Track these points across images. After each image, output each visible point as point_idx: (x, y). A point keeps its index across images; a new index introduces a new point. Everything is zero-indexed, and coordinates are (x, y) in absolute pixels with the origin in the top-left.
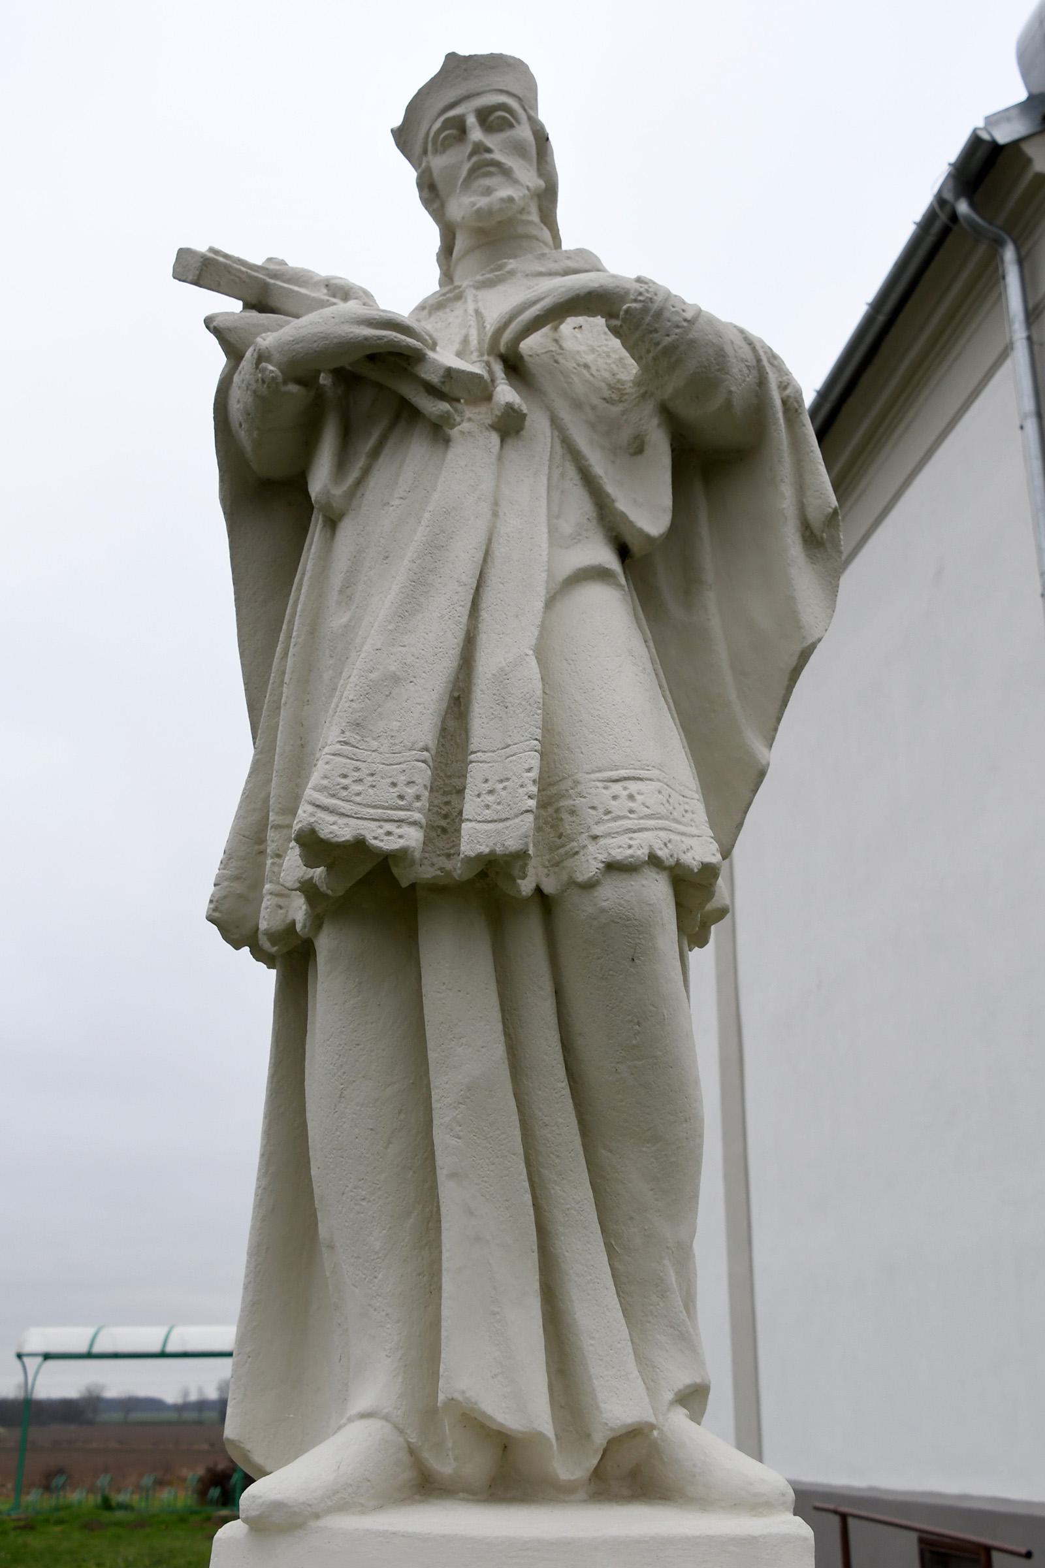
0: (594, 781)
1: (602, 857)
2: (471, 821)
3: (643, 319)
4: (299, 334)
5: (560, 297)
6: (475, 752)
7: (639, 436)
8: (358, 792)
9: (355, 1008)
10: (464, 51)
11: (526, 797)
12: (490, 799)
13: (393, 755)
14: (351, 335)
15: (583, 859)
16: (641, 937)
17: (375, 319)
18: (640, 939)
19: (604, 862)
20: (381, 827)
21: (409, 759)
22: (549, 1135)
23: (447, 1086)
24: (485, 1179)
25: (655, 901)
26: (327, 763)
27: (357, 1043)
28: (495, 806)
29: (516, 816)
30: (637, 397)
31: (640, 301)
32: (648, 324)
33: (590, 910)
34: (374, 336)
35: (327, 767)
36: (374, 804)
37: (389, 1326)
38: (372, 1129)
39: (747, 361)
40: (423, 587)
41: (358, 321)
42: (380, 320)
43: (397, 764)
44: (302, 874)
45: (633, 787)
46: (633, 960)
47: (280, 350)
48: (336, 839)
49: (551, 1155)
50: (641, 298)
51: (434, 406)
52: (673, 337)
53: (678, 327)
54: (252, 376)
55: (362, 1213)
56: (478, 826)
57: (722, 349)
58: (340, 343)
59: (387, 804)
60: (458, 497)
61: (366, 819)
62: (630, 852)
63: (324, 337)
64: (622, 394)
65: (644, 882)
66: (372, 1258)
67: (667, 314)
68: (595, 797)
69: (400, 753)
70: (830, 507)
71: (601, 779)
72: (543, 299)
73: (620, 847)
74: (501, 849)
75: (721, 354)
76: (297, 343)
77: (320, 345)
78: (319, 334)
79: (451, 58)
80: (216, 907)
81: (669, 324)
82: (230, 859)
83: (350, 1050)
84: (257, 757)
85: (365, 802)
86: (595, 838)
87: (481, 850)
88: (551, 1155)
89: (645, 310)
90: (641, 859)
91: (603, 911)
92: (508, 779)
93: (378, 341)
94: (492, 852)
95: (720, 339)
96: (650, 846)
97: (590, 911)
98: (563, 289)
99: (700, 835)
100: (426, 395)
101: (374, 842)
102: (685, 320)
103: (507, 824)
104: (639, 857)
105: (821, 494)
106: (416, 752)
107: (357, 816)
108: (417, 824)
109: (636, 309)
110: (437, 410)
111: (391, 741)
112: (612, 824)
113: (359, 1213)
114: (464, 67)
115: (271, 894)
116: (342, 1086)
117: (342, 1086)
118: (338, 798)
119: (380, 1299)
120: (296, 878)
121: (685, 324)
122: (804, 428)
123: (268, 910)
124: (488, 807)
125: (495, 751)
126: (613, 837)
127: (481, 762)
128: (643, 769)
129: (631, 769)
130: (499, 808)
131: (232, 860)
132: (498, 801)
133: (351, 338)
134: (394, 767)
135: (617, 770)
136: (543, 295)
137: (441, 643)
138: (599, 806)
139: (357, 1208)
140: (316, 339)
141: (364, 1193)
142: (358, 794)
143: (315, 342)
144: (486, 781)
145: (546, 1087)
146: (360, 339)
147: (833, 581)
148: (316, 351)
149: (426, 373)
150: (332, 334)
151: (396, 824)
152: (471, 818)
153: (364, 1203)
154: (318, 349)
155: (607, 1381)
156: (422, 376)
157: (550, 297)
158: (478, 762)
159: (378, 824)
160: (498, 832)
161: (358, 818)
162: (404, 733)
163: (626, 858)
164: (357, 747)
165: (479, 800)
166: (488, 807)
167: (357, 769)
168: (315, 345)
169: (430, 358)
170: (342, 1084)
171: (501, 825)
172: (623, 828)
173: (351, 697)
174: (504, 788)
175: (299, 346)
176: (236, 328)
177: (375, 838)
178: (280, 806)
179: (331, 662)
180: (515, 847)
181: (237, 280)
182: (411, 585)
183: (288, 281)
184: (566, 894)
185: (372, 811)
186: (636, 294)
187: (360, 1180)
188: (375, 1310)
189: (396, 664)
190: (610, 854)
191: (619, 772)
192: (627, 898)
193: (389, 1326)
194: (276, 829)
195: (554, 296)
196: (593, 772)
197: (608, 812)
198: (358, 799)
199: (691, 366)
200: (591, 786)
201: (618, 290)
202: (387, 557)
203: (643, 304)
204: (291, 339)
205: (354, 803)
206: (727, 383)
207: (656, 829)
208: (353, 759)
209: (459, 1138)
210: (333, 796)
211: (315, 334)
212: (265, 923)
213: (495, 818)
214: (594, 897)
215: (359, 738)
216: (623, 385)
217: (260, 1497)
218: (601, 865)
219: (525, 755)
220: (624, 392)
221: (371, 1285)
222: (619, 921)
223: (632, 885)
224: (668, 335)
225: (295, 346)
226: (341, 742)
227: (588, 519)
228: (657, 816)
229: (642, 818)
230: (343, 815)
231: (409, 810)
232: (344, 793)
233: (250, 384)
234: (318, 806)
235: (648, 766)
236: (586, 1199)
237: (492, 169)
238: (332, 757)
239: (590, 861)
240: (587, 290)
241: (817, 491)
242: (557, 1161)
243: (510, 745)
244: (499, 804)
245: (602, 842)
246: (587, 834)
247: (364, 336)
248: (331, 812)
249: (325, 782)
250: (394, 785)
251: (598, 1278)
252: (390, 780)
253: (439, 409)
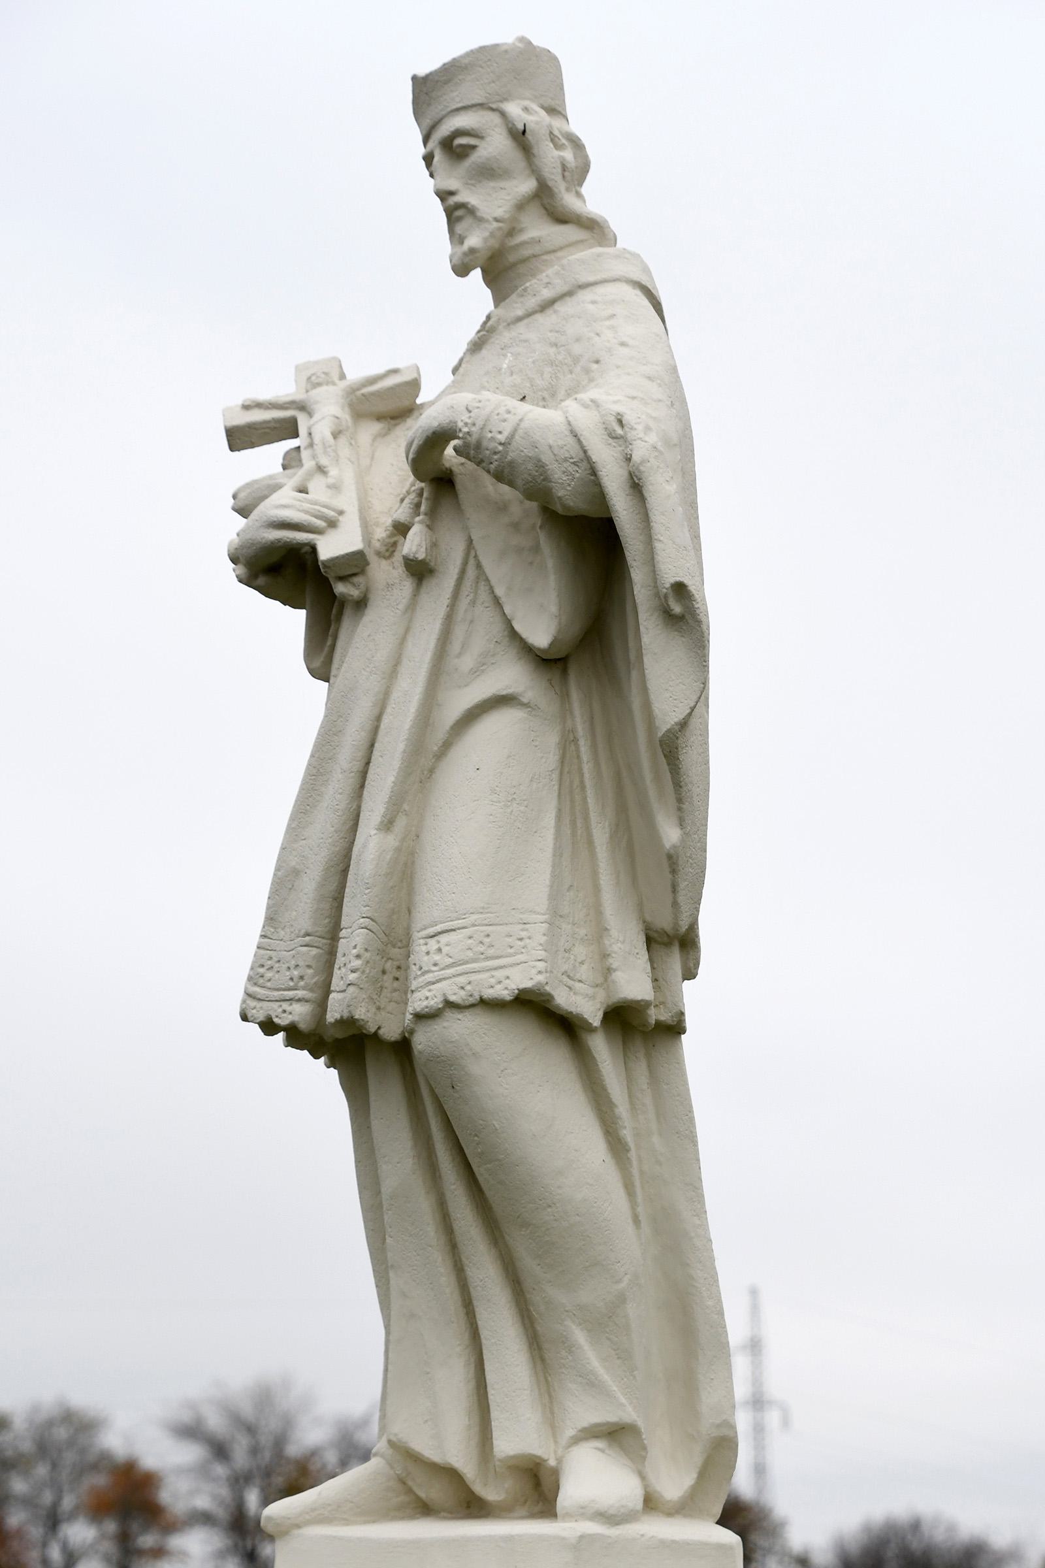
14: (264, 541)
16: (452, 1068)
17: (275, 522)
24: (415, 1268)
25: (457, 1038)
39: (572, 458)
45: (444, 939)
46: (453, 1087)
53: (495, 453)
57: (539, 461)
59: (283, 987)
60: (355, 676)
62: (425, 1003)
65: (445, 1024)
67: (485, 443)
70: (664, 588)
71: (424, 936)
73: (420, 1000)
75: (540, 465)
81: (488, 452)
85: (273, 986)
95: (536, 450)
102: (500, 444)
104: (432, 1007)
121: (500, 448)
128: (459, 919)
129: (448, 921)
135: (436, 925)
147: (699, 652)
151: (288, 1003)
155: (501, 1422)
161: (268, 1001)
163: (423, 1009)
164: (271, 939)
167: (270, 958)
172: (425, 982)
176: (247, 506)
177: (277, 1017)
181: (267, 430)
189: (296, 858)
191: (437, 927)
196: (422, 930)
198: (269, 984)
201: (451, 425)
207: (454, 976)
208: (268, 950)
215: (272, 930)
222: (432, 1059)
223: (435, 1029)
224: (491, 463)
227: (496, 642)
228: (459, 963)
229: (443, 969)
230: (260, 1000)
231: (296, 989)
232: (261, 981)
236: (487, 1277)
240: (431, 431)
251: (499, 1341)
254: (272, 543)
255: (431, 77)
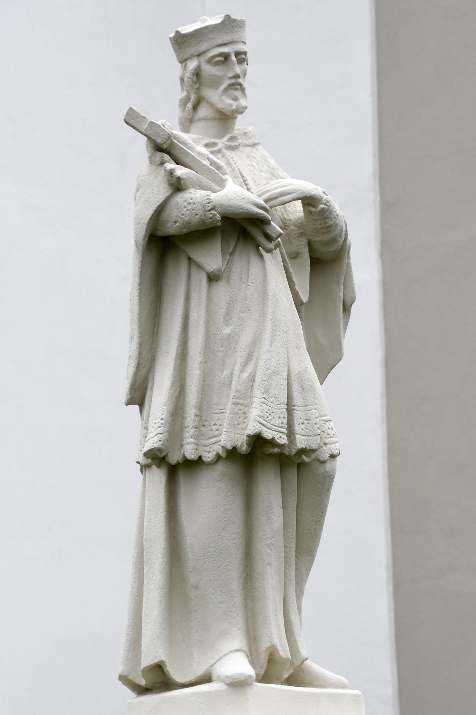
0: (322, 420)
1: (329, 452)
2: (298, 434)
3: (326, 213)
4: (230, 202)
5: (300, 195)
6: (295, 406)
7: (298, 252)
9: (231, 495)
10: (233, 17)
12: (303, 426)
13: (278, 405)
14: (252, 210)
15: (322, 452)
17: (259, 204)
19: (330, 454)
20: (278, 434)
21: (283, 408)
22: (288, 551)
23: (268, 530)
26: (261, 406)
27: (231, 509)
28: (305, 430)
29: (315, 436)
30: (298, 233)
31: (327, 205)
32: (327, 215)
33: (322, 471)
34: (260, 213)
35: (261, 408)
36: (275, 425)
37: (238, 618)
38: (235, 544)
41: (253, 204)
42: (261, 205)
43: (279, 409)
44: (233, 444)
46: (328, 490)
47: (221, 207)
48: (268, 438)
49: (288, 559)
50: (328, 204)
51: (268, 245)
52: (333, 222)
54: (203, 212)
55: (229, 575)
56: (301, 437)
58: (246, 212)
59: (279, 425)
61: (274, 430)
63: (242, 208)
64: (285, 225)
66: (232, 593)
67: (333, 212)
68: (323, 427)
69: (279, 405)
71: (324, 420)
72: (294, 193)
74: (309, 447)
76: (230, 207)
77: (239, 211)
78: (240, 206)
79: (227, 17)
80: (163, 444)
81: (333, 216)
82: (166, 423)
83: (229, 512)
84: (173, 379)
85: (273, 424)
86: (325, 444)
87: (302, 447)
88: (288, 559)
89: (328, 209)
91: (326, 472)
92: (309, 420)
93: (260, 216)
94: (306, 448)
97: (322, 471)
98: (301, 191)
100: (264, 238)
101: (277, 440)
103: (312, 438)
105: (354, 292)
107: (272, 429)
109: (325, 209)
110: (269, 247)
111: (276, 399)
112: (330, 439)
113: (227, 575)
114: (232, 25)
115: (194, 443)
116: (224, 526)
117: (224, 526)
118: (266, 421)
119: (234, 608)
120: (231, 445)
122: (349, 260)
123: (194, 450)
124: (303, 429)
125: (301, 407)
126: (331, 445)
127: (298, 410)
130: (307, 431)
131: (167, 424)
132: (306, 428)
133: (251, 212)
134: (279, 410)
136: (292, 192)
137: (284, 359)
138: (325, 431)
139: (227, 573)
140: (238, 208)
141: (230, 568)
142: (271, 420)
143: (238, 209)
144: (300, 419)
145: (289, 533)
146: (255, 213)
148: (237, 213)
149: (269, 231)
150: (245, 207)
152: (298, 433)
153: (230, 571)
154: (238, 212)
156: (268, 231)
157: (296, 193)
158: (297, 410)
160: (308, 440)
161: (272, 430)
162: (279, 396)
165: (299, 426)
166: (303, 429)
168: (237, 210)
169: (272, 225)
170: (224, 525)
171: (308, 438)
173: (264, 379)
174: (308, 423)
175: (230, 208)
176: (185, 178)
177: (277, 439)
178: (198, 407)
179: (222, 349)
180: (315, 448)
183: (181, 143)
184: (312, 463)
186: (326, 202)
187: (229, 563)
188: (232, 612)
190: (332, 451)
193: (238, 618)
194: (196, 416)
195: (297, 194)
197: (328, 434)
199: (333, 234)
200: (321, 422)
201: (319, 197)
202: (250, 310)
203: (328, 207)
204: (227, 204)
205: (270, 423)
206: (340, 242)
209: (272, 550)
210: (265, 420)
211: (238, 206)
212: (193, 456)
213: (306, 435)
214: (325, 467)
216: (286, 221)
217: (244, 674)
218: (329, 455)
219: (315, 411)
220: (286, 224)
221: (230, 603)
224: (331, 221)
225: (228, 208)
226: (263, 398)
233: (202, 216)
234: (261, 424)
237: (238, 87)
238: (262, 404)
239: (325, 453)
240: (310, 195)
241: (352, 290)
242: (289, 561)
243: (307, 406)
244: (307, 429)
245: (329, 446)
246: (322, 442)
247: (256, 212)
248: (265, 427)
249: (262, 414)
250: (279, 418)
252: (278, 416)
253: (270, 247)
254: (257, 213)
255: (237, 21)
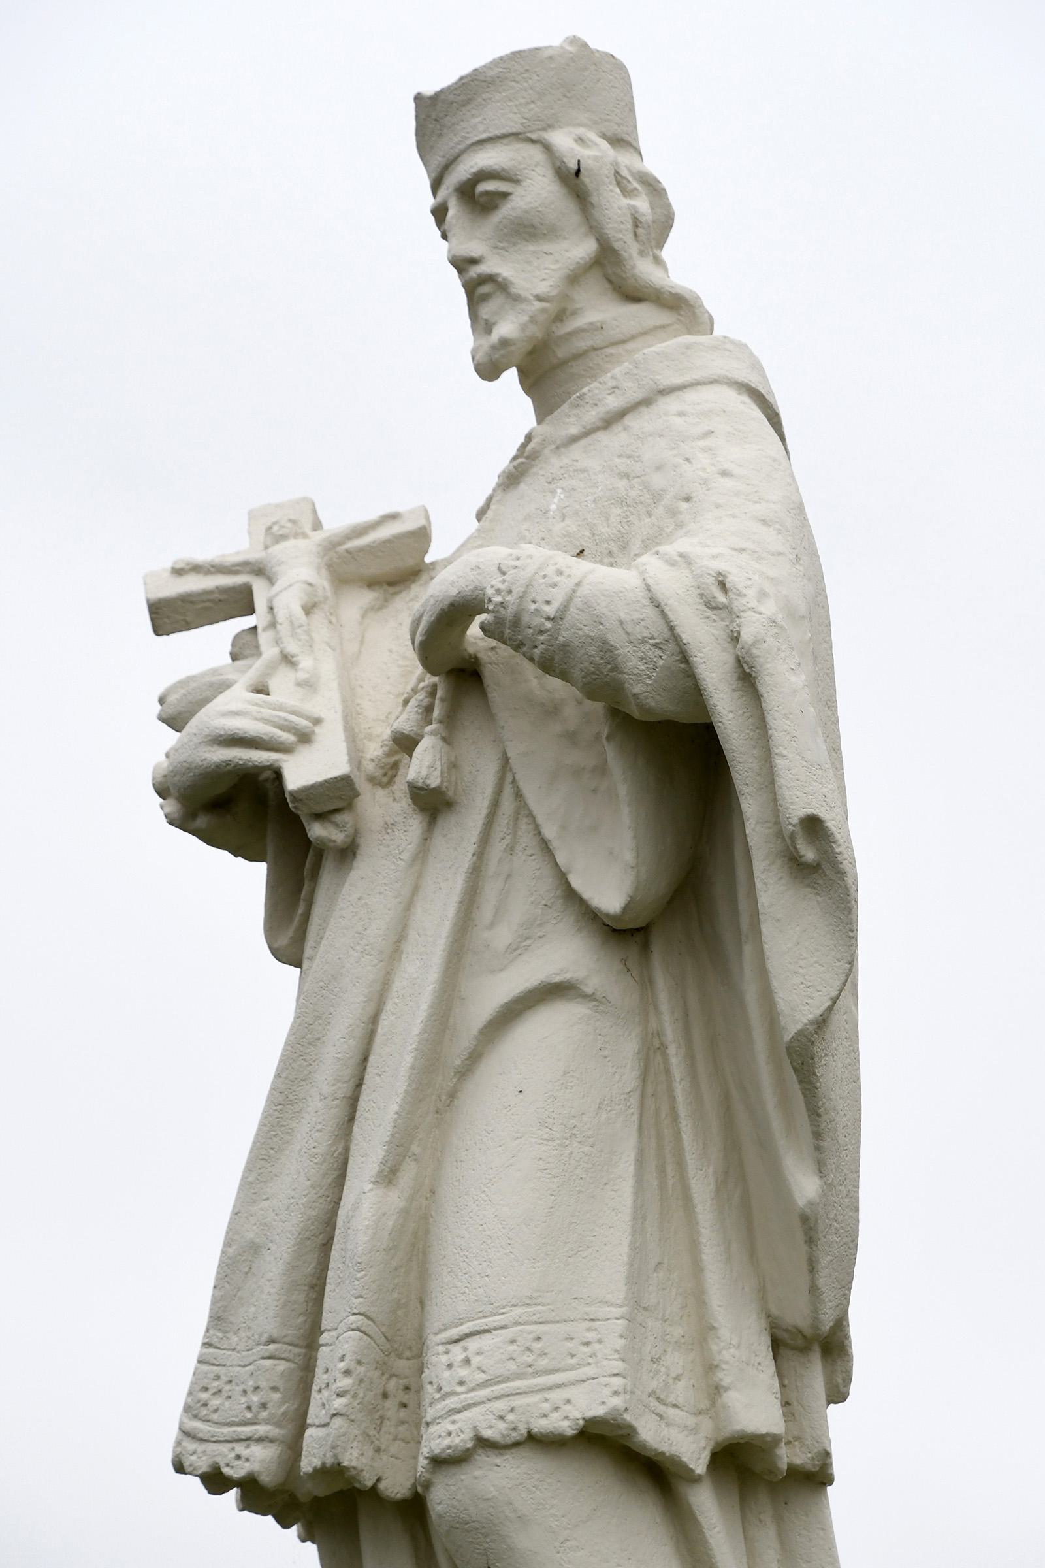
8: (215, 1407)
11: (335, 1396)
16: (488, 1540)
17: (221, 736)
18: (487, 1543)
36: (228, 1420)
40: (295, 1106)
45: (473, 1344)
53: (541, 632)
59: (237, 1420)
62: (447, 1441)
65: (477, 1473)
67: (526, 619)
71: (444, 1341)
85: (221, 1420)
90: (459, 1448)
95: (601, 627)
96: (475, 1427)
99: (595, 1376)
102: (548, 619)
104: (457, 1446)
106: (262, 1347)
107: (213, 1439)
108: (263, 1440)
114: (434, 115)
121: (548, 625)
129: (480, 1318)
135: (462, 1324)
151: (244, 1444)
159: (229, 1445)
161: (214, 1442)
163: (443, 1450)
172: (447, 1409)
177: (227, 1465)
182: (276, 1110)
185: (226, 1430)
192: (459, 1497)
198: (215, 1417)
208: (213, 1365)
215: (220, 1335)
222: (458, 1525)
228: (497, 1380)
229: (473, 1389)
230: (202, 1440)
231: (255, 1424)
232: (204, 1412)
235: (504, 1308)
255: (442, 97)
